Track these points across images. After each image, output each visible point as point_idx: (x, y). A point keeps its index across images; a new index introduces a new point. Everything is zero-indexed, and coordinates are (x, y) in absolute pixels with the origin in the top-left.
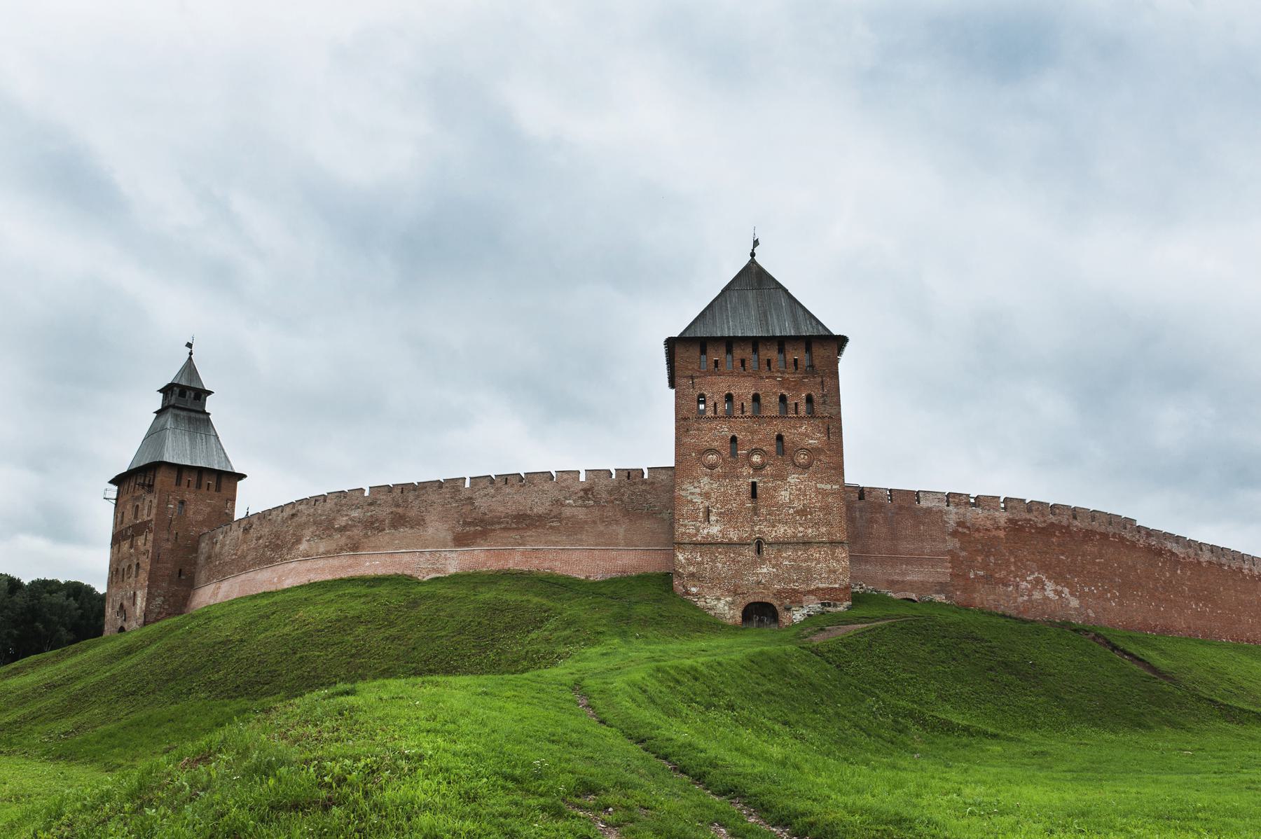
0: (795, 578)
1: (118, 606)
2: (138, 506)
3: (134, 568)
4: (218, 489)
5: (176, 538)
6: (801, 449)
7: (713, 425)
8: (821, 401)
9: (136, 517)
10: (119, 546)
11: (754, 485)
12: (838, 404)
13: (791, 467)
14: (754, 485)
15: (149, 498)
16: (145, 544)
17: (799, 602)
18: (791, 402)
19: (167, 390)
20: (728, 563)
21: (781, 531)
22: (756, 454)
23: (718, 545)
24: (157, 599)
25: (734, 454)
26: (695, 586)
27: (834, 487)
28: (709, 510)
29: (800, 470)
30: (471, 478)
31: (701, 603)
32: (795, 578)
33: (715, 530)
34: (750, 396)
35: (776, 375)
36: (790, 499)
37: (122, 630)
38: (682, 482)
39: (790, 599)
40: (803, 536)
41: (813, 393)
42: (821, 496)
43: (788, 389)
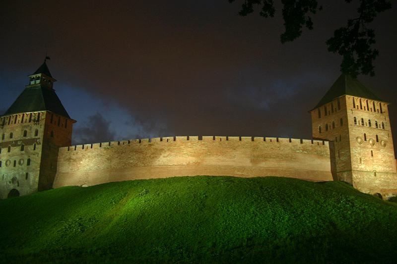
3: (26, 161)
9: (25, 135)
15: (35, 127)
16: (34, 149)
18: (378, 124)
43: (377, 119)
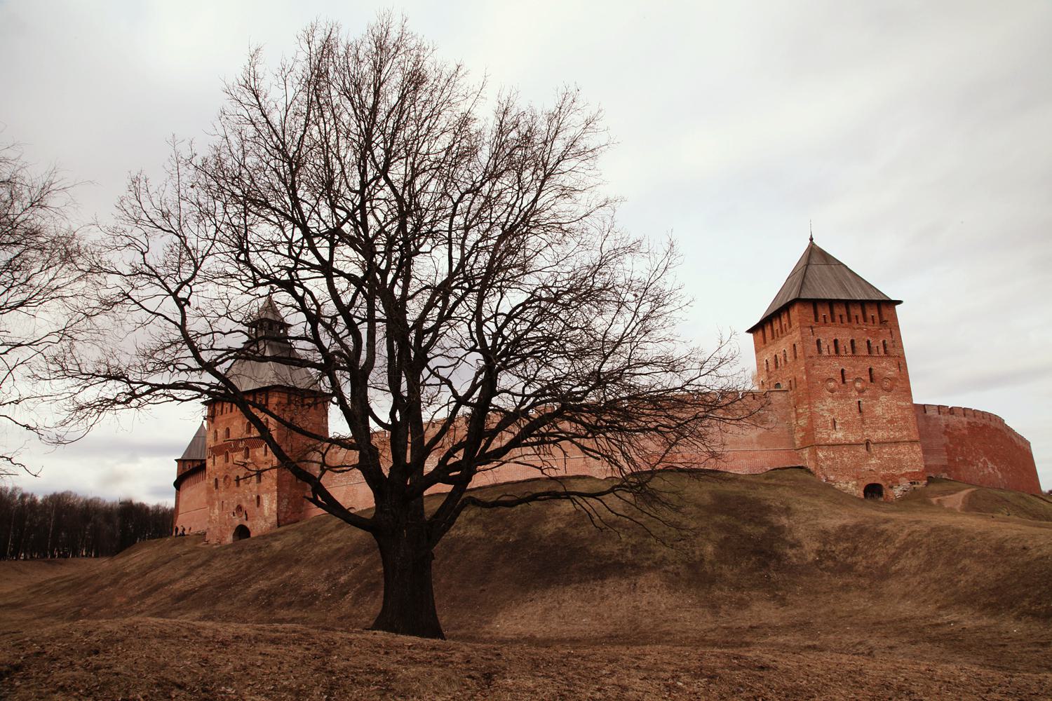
7: (829, 362)
8: (892, 345)
12: (902, 347)
13: (880, 391)
14: (859, 402)
18: (874, 346)
21: (880, 435)
25: (844, 382)
26: (832, 475)
31: (837, 486)
33: (839, 435)
34: (849, 341)
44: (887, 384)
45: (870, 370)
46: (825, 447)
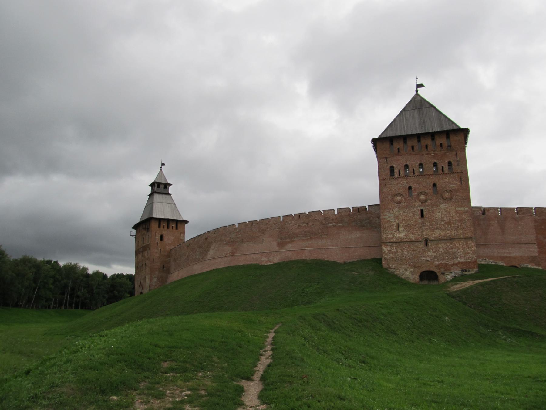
0: (446, 257)
1: (139, 283)
2: (144, 238)
3: (144, 266)
4: (177, 228)
5: (160, 251)
6: (446, 190)
8: (456, 164)
9: (143, 243)
10: (138, 256)
11: (422, 211)
13: (441, 200)
14: (422, 211)
16: (148, 255)
17: (449, 270)
18: (440, 166)
19: (152, 185)
20: (410, 252)
21: (437, 234)
22: (422, 195)
23: (404, 243)
24: (154, 279)
25: (410, 195)
27: (466, 209)
28: (399, 225)
29: (446, 201)
30: (283, 216)
32: (446, 257)
33: (402, 235)
35: (431, 152)
36: (441, 217)
37: (141, 293)
38: (384, 211)
39: (444, 268)
40: (450, 235)
41: (452, 161)
42: (458, 214)
43: (438, 159)
44: (447, 195)
45: (435, 185)
46: (389, 244)
